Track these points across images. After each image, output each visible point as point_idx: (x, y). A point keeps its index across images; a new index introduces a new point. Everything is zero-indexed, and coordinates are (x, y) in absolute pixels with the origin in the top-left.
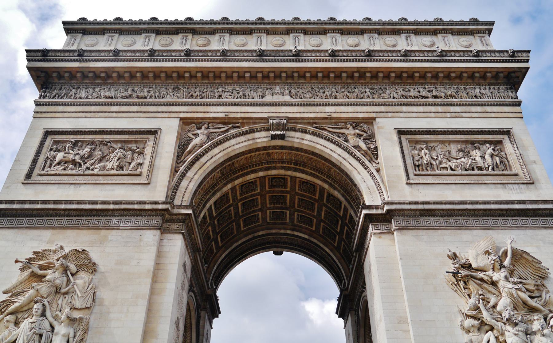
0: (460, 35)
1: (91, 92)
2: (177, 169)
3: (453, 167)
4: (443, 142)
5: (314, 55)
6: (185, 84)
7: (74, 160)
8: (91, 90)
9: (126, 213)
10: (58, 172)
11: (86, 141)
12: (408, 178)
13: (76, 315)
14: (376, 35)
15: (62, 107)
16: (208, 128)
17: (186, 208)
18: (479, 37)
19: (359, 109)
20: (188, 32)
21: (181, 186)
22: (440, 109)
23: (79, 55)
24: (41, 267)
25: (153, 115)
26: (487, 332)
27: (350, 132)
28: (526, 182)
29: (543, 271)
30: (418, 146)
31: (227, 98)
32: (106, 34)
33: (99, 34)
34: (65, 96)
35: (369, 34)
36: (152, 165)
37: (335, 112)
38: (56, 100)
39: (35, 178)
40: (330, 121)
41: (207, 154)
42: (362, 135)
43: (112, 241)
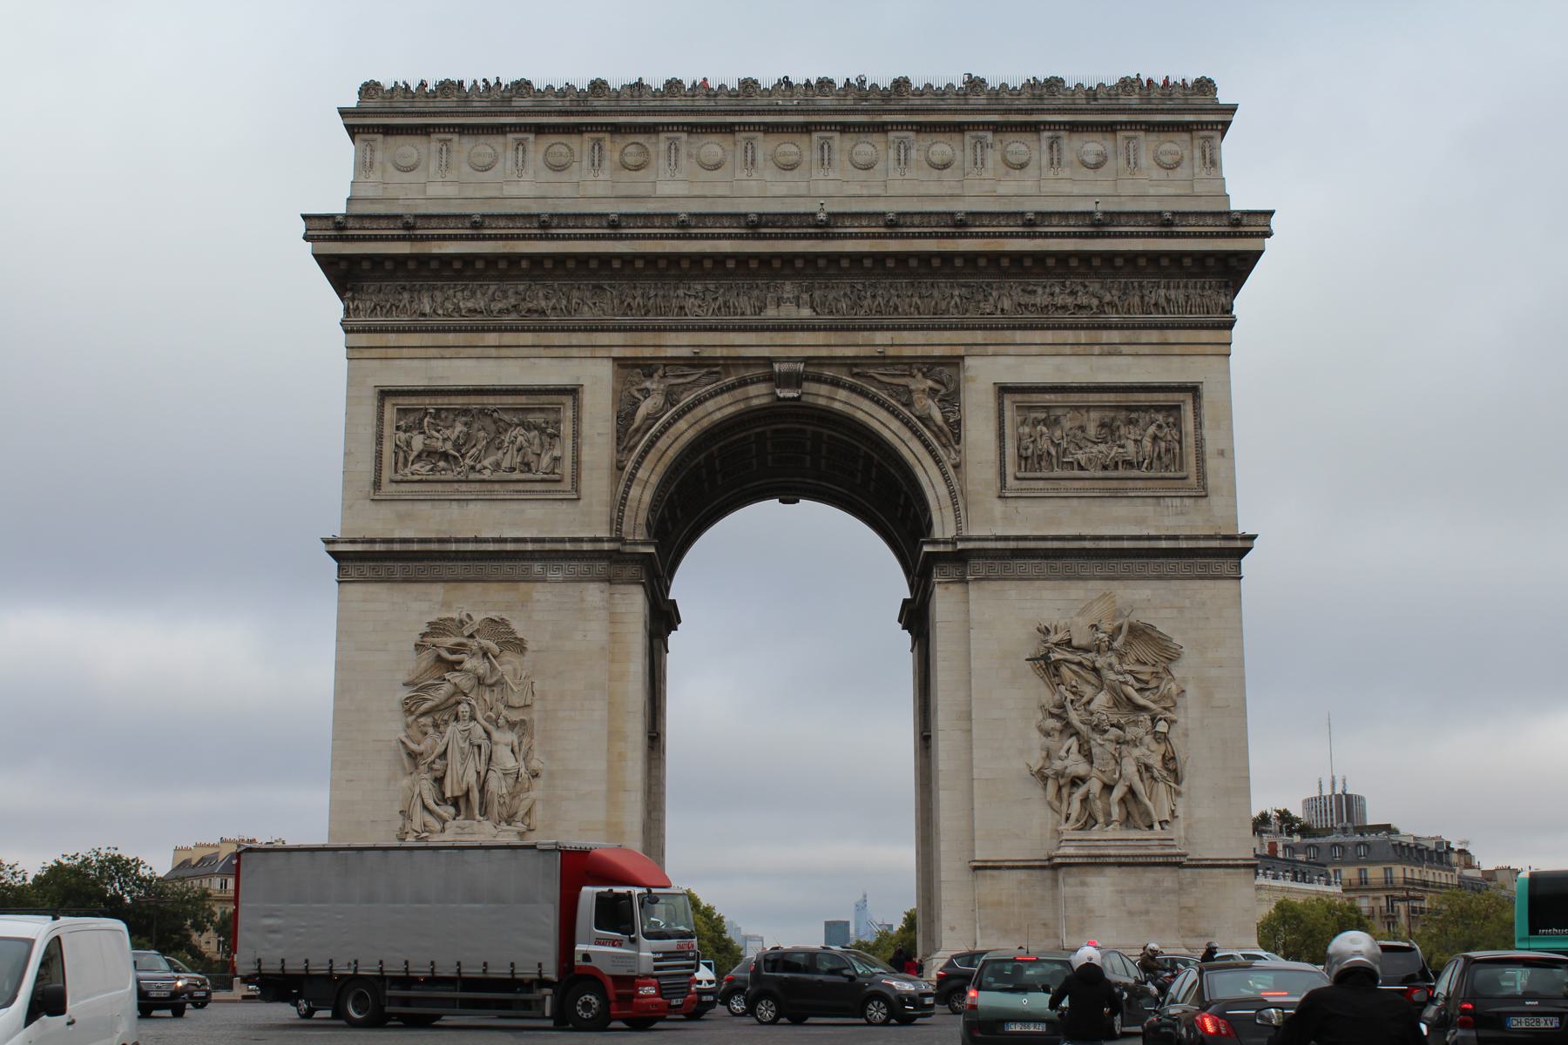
0: (1163, 131)
1: (439, 300)
2: (620, 465)
3: (1083, 464)
4: (1077, 408)
5: (856, 224)
6: (611, 277)
7: (444, 452)
8: (437, 293)
9: (553, 555)
10: (424, 478)
11: (455, 409)
12: (1003, 486)
13: (515, 716)
14: (989, 136)
15: (394, 335)
16: (664, 376)
17: (644, 543)
18: (1202, 138)
19: (936, 336)
20: (601, 131)
21: (630, 497)
22: (1083, 336)
23: (408, 227)
24: (452, 651)
25: (563, 353)
26: (1071, 736)
27: (920, 384)
28: (1194, 494)
29: (1174, 651)
30: (1033, 415)
31: (696, 309)
32: (432, 136)
33: (417, 134)
34: (394, 309)
35: (974, 134)
36: (577, 462)
37: (892, 345)
38: (379, 320)
39: (388, 489)
40: (881, 361)
41: (668, 433)
42: (939, 391)
43: (539, 601)
